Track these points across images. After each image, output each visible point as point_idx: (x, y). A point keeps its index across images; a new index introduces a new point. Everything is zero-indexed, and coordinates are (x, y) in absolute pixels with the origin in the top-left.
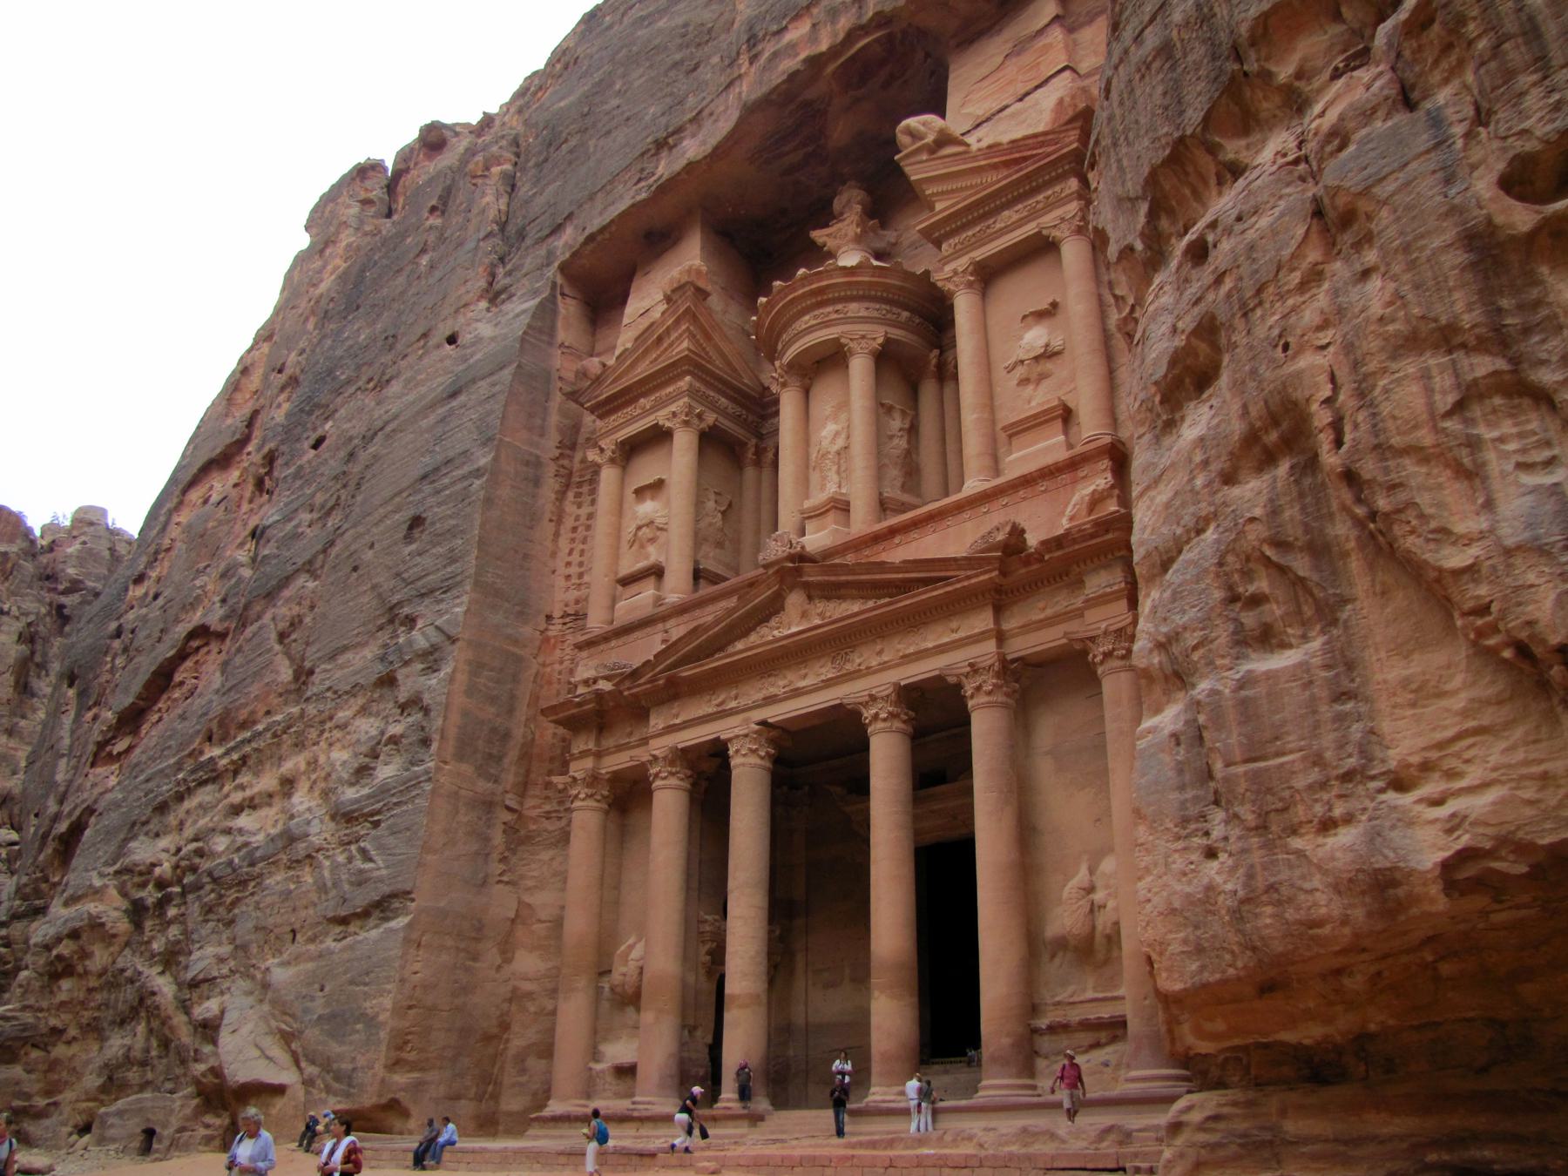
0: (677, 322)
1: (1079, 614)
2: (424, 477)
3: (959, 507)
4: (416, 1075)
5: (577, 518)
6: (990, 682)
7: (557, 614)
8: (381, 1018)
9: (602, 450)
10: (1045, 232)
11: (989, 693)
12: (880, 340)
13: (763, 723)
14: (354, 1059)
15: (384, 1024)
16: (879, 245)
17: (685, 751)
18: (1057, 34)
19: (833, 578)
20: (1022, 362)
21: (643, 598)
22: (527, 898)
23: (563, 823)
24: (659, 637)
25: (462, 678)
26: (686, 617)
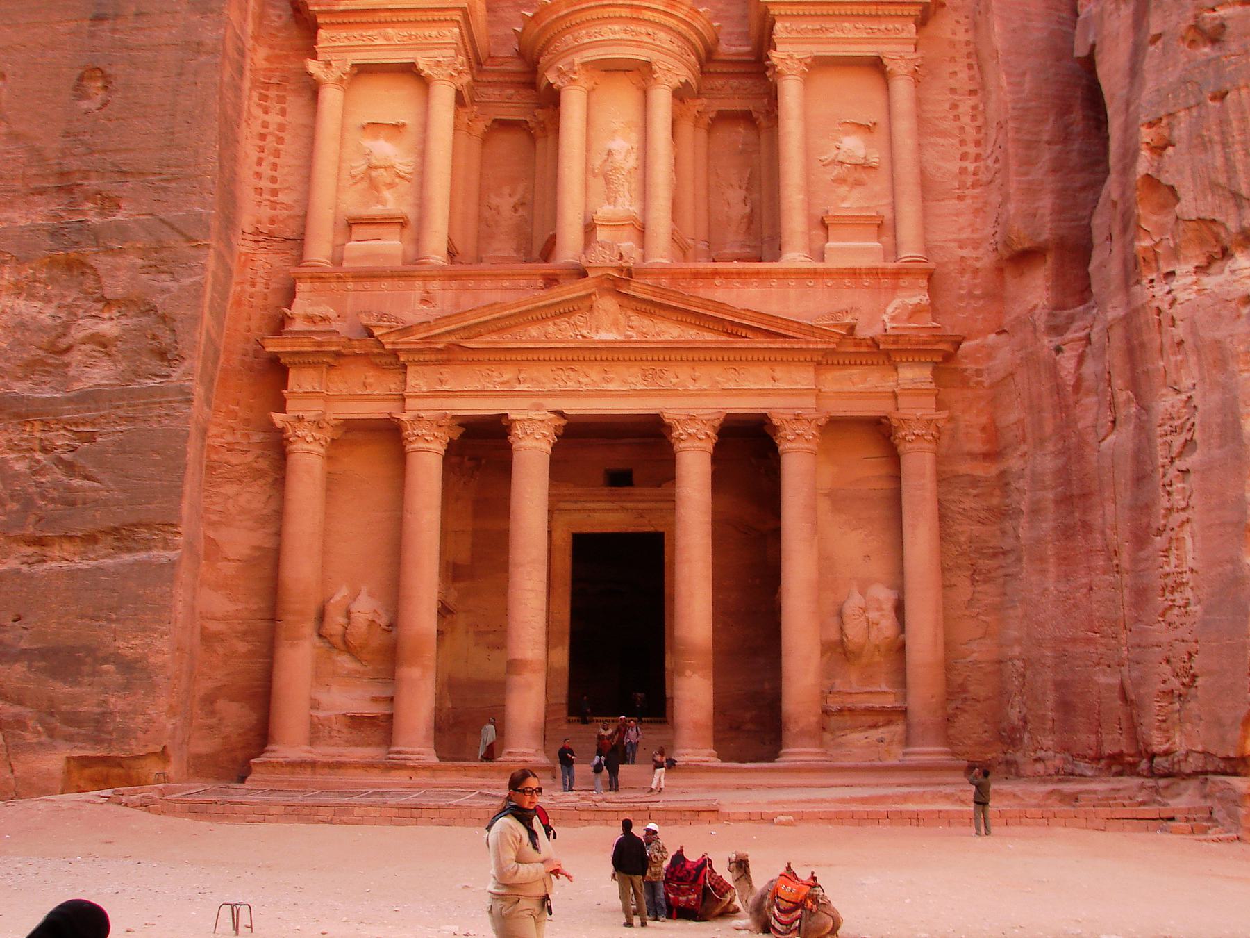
1: (895, 396)
3: (786, 274)
4: (173, 721)
5: (265, 125)
6: (810, 432)
7: (249, 229)
8: (152, 659)
9: (328, 64)
10: (885, 61)
12: (683, 80)
13: (560, 413)
14: (105, 702)
15: (163, 667)
17: (454, 417)
20: (842, 163)
22: (211, 534)
24: (417, 295)
26: (454, 284)
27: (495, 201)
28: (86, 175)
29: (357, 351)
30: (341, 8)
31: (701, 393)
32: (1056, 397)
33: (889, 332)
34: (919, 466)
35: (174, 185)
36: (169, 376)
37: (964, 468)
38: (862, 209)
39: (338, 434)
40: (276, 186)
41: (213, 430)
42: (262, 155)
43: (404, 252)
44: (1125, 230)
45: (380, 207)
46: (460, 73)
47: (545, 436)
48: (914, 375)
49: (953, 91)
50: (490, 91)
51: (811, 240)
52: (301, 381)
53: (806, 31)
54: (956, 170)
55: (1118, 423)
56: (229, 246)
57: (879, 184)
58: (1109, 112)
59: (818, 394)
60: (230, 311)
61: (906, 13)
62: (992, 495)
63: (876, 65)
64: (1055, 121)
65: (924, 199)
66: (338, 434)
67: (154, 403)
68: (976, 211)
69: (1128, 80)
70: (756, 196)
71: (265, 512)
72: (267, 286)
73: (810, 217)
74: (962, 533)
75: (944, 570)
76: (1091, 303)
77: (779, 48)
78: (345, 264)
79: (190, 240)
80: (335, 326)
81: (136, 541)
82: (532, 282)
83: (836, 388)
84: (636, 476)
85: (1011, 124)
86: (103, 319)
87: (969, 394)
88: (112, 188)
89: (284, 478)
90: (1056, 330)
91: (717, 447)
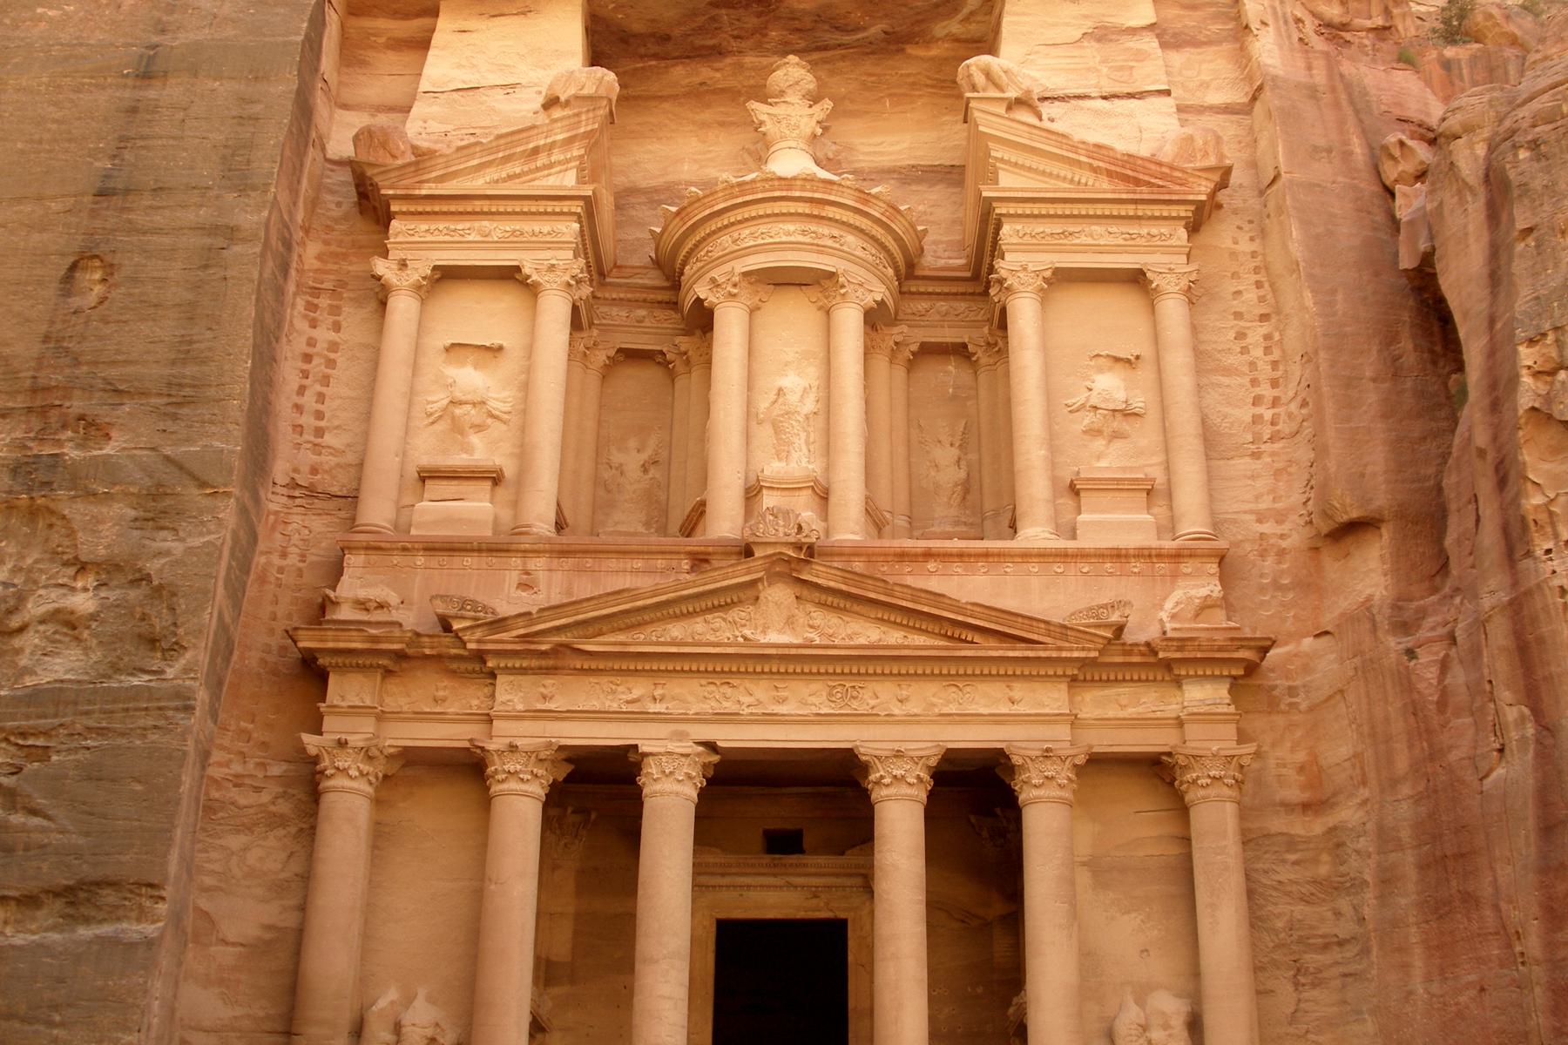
0: (569, 141)
2: (102, 193)
3: (1026, 556)
6: (1064, 774)
7: (281, 479)
9: (403, 264)
10: (1149, 275)
11: (1061, 786)
13: (711, 746)
16: (820, 155)
17: (562, 748)
18: (1150, 43)
19: (853, 590)
20: (1095, 408)
21: (475, 510)
23: (265, 797)
24: (514, 577)
25: (226, 553)
27: (617, 457)
28: (67, 390)
29: (427, 651)
30: (424, 192)
31: (912, 720)
32: (1412, 720)
33: (1170, 634)
34: (1216, 819)
35: (184, 411)
36: (162, 672)
37: (1277, 823)
38: (1124, 469)
39: (394, 768)
40: (322, 424)
41: (217, 756)
42: (305, 382)
43: (496, 518)
44: (1502, 483)
45: (464, 456)
46: (579, 282)
47: (689, 777)
48: (1206, 695)
49: (1238, 315)
50: (615, 311)
51: (1056, 511)
52: (344, 690)
53: (1043, 235)
54: (1248, 419)
55: (1507, 751)
56: (257, 500)
57: (1146, 436)
58: (1462, 335)
59: (1074, 721)
60: (251, 591)
61: (1174, 214)
62: (1315, 861)
63: (1136, 279)
64: (1379, 351)
65: (1208, 458)
66: (394, 768)
67: (136, 709)
68: (1277, 473)
69: (1487, 291)
70: (973, 456)
71: (282, 876)
72: (303, 558)
73: (1054, 480)
74: (1279, 916)
75: (1257, 969)
76: (1447, 590)
77: (1008, 256)
78: (413, 532)
79: (203, 484)
80: (395, 616)
81: (99, 908)
82: (674, 563)
83: (1098, 713)
84: (807, 840)
85: (1322, 354)
86: (73, 589)
87: (1280, 720)
88: (103, 413)
89: (313, 828)
90: (1403, 627)
91: (931, 795)
